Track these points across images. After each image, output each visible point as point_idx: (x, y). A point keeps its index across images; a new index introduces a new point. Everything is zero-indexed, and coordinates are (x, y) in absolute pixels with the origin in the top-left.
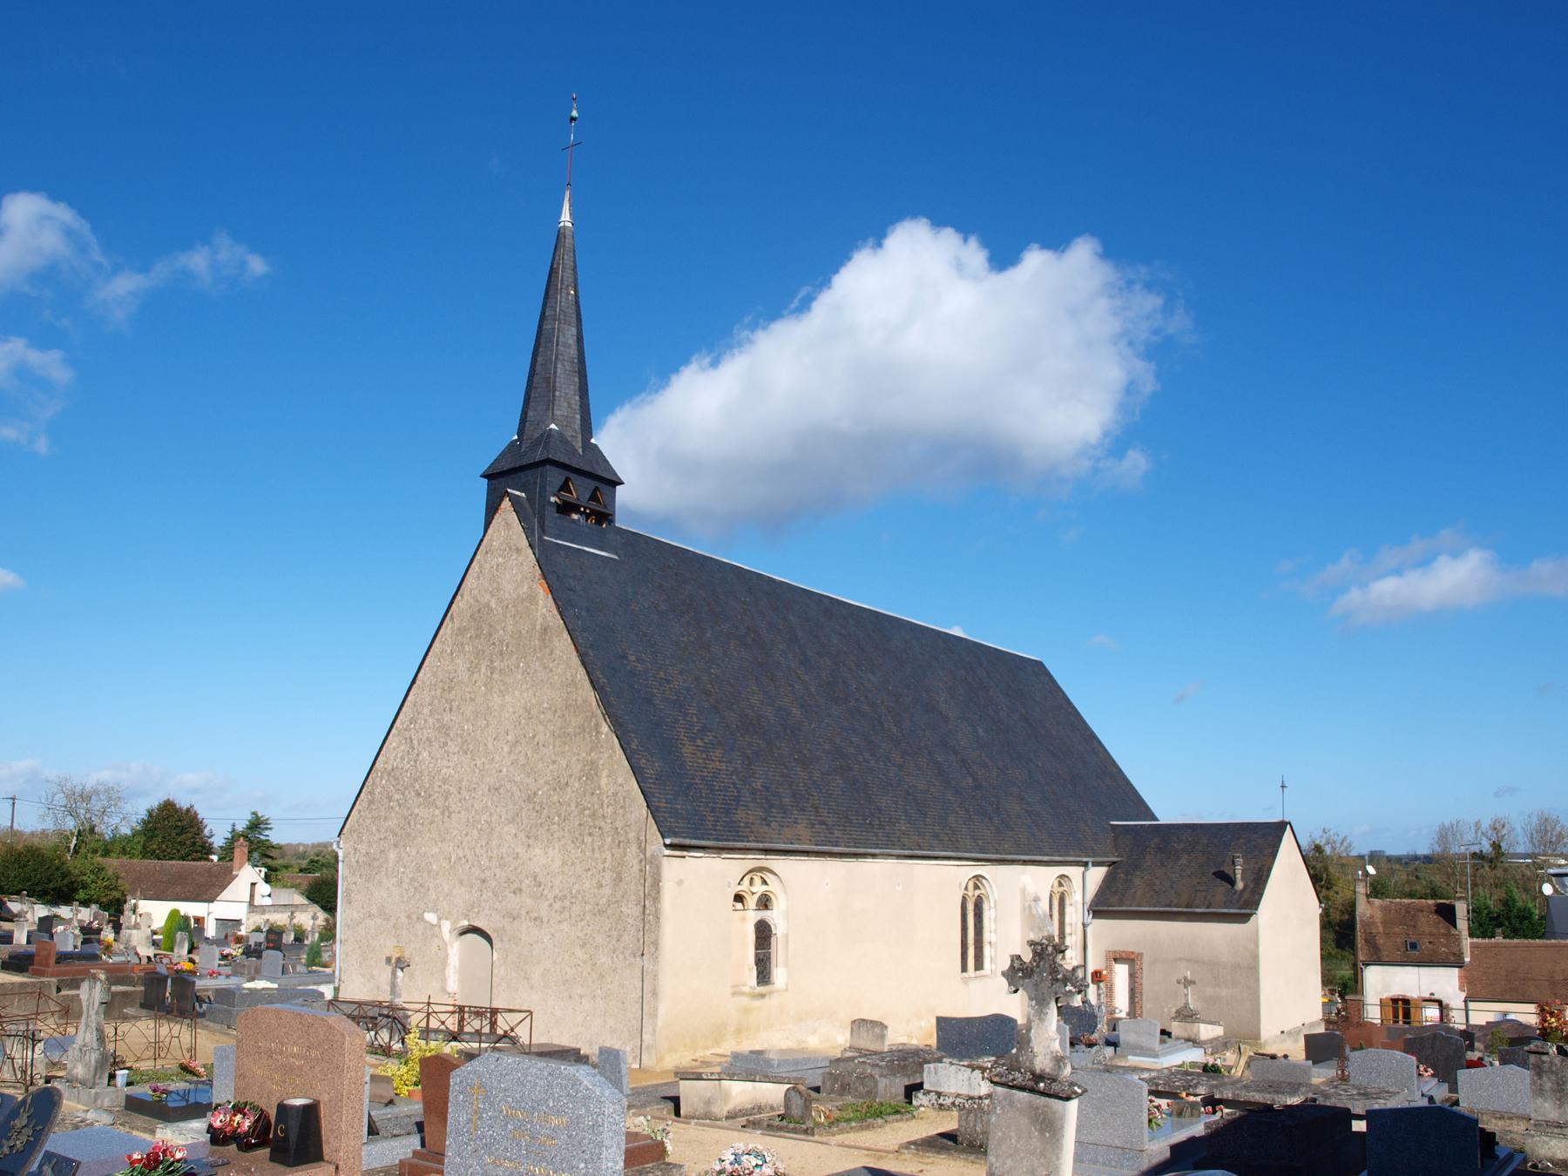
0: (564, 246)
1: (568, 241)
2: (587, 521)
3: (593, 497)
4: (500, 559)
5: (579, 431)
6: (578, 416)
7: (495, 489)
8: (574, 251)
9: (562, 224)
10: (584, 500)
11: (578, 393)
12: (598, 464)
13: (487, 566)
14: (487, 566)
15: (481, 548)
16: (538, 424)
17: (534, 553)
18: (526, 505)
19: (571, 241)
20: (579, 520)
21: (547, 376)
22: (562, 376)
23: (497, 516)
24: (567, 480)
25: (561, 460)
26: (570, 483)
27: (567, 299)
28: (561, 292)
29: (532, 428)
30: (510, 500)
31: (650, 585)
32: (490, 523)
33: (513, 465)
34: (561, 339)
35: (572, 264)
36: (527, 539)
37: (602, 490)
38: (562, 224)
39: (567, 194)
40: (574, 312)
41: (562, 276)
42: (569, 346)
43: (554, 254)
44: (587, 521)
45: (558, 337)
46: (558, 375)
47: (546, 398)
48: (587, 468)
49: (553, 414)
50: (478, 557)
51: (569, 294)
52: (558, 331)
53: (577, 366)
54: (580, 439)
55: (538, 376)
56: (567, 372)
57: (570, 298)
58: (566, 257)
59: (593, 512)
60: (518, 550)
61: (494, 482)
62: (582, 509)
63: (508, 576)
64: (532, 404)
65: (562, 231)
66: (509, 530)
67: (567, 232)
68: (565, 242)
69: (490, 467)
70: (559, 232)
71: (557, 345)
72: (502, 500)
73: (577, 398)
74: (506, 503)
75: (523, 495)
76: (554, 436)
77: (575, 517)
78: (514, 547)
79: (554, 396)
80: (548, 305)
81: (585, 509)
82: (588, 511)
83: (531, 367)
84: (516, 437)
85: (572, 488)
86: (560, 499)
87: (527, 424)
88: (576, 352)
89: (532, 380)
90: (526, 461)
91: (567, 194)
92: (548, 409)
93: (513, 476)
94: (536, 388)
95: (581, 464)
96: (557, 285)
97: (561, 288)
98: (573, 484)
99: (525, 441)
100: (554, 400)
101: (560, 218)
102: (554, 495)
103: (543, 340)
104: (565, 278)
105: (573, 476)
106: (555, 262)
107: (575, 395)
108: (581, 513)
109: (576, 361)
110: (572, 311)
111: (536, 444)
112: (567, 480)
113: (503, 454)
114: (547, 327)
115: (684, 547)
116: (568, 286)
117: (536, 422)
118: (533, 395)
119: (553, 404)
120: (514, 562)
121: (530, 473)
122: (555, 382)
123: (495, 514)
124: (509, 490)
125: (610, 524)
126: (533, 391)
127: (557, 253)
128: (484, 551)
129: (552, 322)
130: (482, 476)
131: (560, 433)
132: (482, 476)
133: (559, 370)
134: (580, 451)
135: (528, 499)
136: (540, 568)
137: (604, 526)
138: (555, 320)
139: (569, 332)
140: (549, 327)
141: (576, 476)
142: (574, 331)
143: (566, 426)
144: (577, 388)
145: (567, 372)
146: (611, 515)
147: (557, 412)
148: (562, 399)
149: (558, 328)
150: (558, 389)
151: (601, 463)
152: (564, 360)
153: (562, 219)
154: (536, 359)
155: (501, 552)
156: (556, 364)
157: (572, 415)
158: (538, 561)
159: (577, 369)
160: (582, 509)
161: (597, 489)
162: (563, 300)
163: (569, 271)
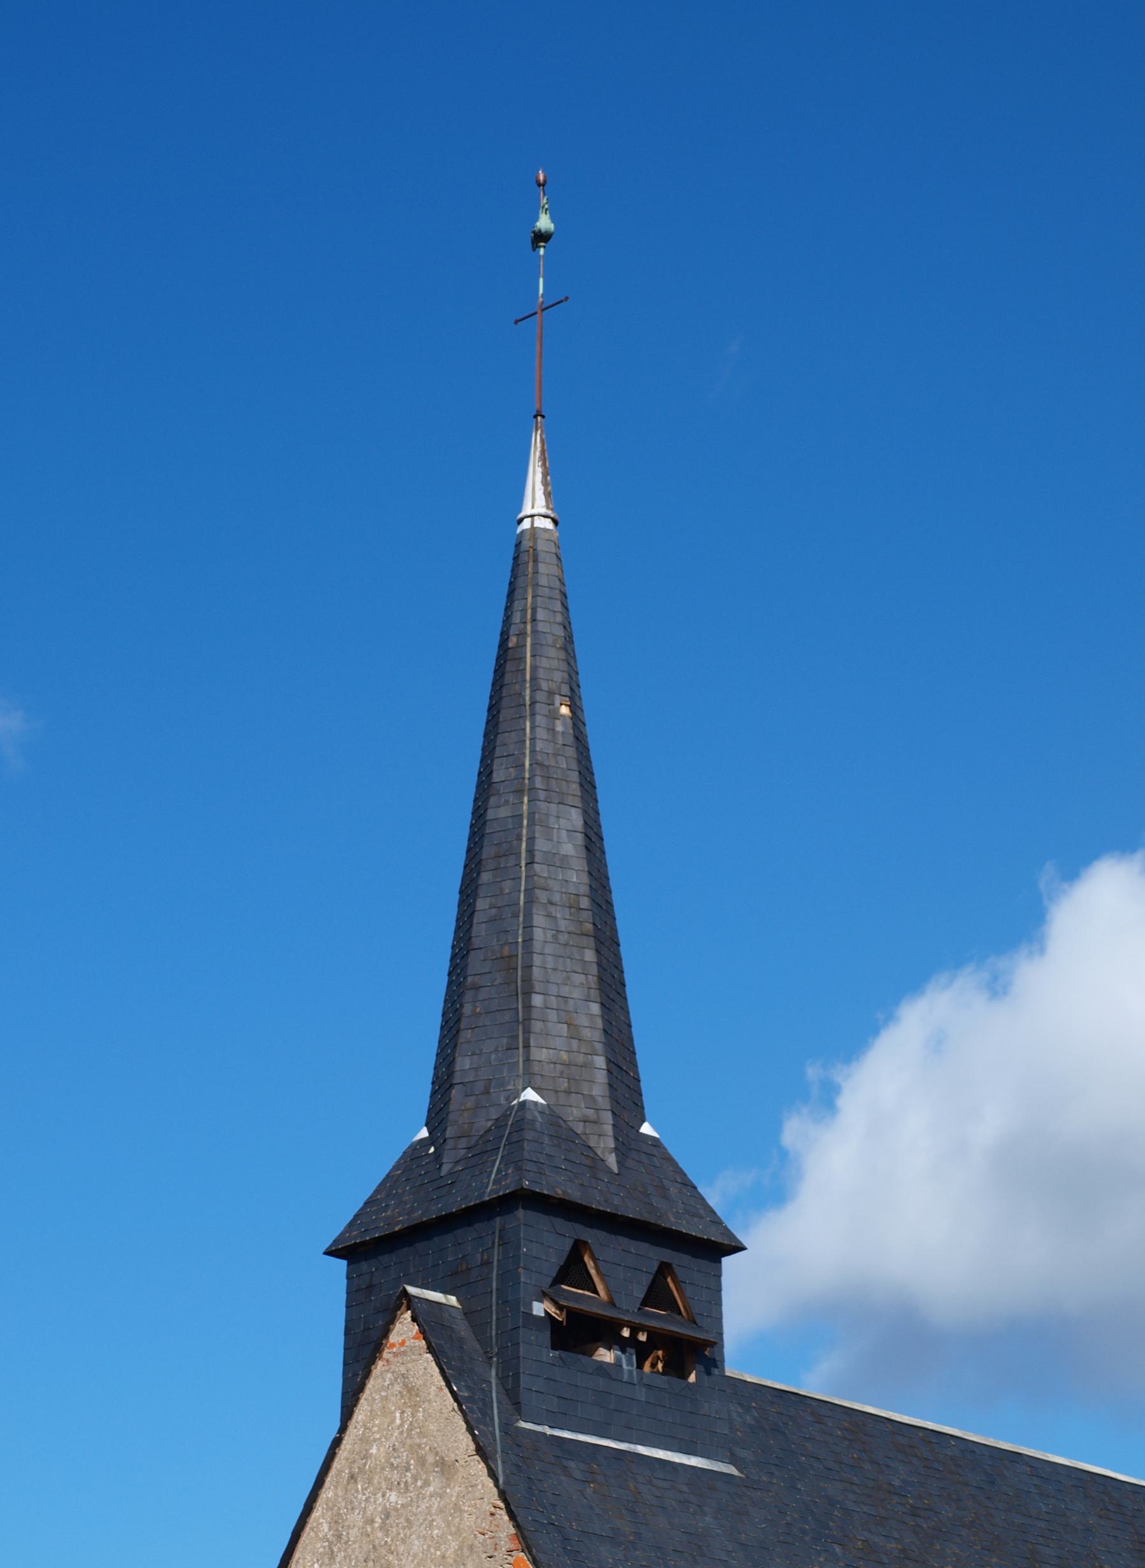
0: (536, 585)
1: (546, 570)
2: (640, 1366)
3: (657, 1295)
4: (393, 1497)
5: (604, 1103)
6: (600, 1062)
7: (370, 1287)
8: (564, 595)
9: (526, 524)
10: (629, 1305)
11: (594, 994)
12: (665, 1197)
13: (356, 1518)
14: (356, 1518)
15: (336, 1465)
16: (487, 1092)
17: (492, 1474)
18: (462, 1328)
19: (554, 570)
20: (618, 1364)
21: (506, 951)
22: (549, 949)
23: (379, 1367)
24: (578, 1249)
25: (559, 1193)
26: (586, 1258)
27: (552, 730)
28: (533, 715)
29: (470, 1102)
30: (414, 1319)
31: (838, 1549)
32: (361, 1388)
33: (419, 1216)
34: (541, 845)
35: (560, 632)
36: (470, 1429)
37: (677, 1270)
38: (526, 524)
39: (536, 440)
40: (574, 765)
41: (534, 669)
42: (563, 863)
43: (508, 608)
44: (640, 1366)
45: (531, 840)
46: (537, 946)
47: (508, 1016)
48: (632, 1210)
49: (527, 1060)
50: (327, 1493)
51: (554, 715)
52: (531, 823)
53: (586, 916)
54: (608, 1129)
55: (481, 955)
56: (563, 938)
57: (559, 728)
58: (541, 615)
59: (658, 1339)
60: (445, 1467)
61: (364, 1266)
62: (626, 1333)
63: (417, 1545)
64: (466, 1035)
65: (526, 544)
66: (415, 1407)
67: (541, 546)
68: (536, 572)
69: (351, 1224)
70: (518, 545)
71: (530, 863)
72: (392, 1320)
73: (595, 1008)
74: (404, 1329)
75: (453, 1300)
76: (534, 1121)
77: (606, 1356)
78: (431, 1459)
79: (528, 1007)
80: (498, 752)
81: (635, 1331)
82: (643, 1337)
83: (458, 928)
84: (424, 1133)
85: (593, 1272)
86: (560, 1307)
87: (455, 1093)
88: (585, 878)
89: (464, 968)
90: (456, 1202)
91: (536, 440)
92: (512, 1048)
93: (420, 1246)
94: (476, 988)
95: (616, 1201)
96: (521, 695)
97: (533, 703)
98: (594, 1259)
99: (450, 1144)
100: (528, 1019)
101: (520, 508)
102: (543, 1296)
103: (488, 851)
104: (541, 674)
105: (591, 1236)
106: (513, 630)
107: (587, 1000)
108: (623, 1345)
109: (585, 903)
110: (565, 764)
111: (480, 1152)
112: (578, 1249)
113: (389, 1185)
114: (498, 812)
115: (930, 1425)
116: (551, 693)
117: (479, 1087)
118: (467, 1009)
119: (527, 1031)
120: (436, 1503)
121: (467, 1234)
122: (528, 967)
123: (372, 1360)
124: (412, 1290)
125: (709, 1373)
126: (469, 996)
127: (518, 605)
128: (346, 1474)
129: (511, 798)
130: (329, 1253)
131: (552, 1116)
132: (329, 1253)
133: (538, 934)
134: (612, 1161)
135: (467, 1313)
136: (512, 1516)
137: (692, 1378)
138: (519, 792)
139: (563, 822)
140: (504, 812)
141: (601, 1235)
142: (575, 818)
143: (568, 1092)
144: (593, 980)
145: (563, 938)
146: (712, 1344)
147: (540, 1054)
148: (552, 1015)
149: (531, 815)
150: (538, 987)
151: (673, 1191)
152: (551, 903)
153: (527, 510)
154: (472, 906)
155: (395, 1476)
156: (529, 916)
157: (580, 1059)
158: (502, 1495)
159: (589, 927)
160: (626, 1333)
161: (665, 1269)
162: (541, 733)
163: (552, 653)
